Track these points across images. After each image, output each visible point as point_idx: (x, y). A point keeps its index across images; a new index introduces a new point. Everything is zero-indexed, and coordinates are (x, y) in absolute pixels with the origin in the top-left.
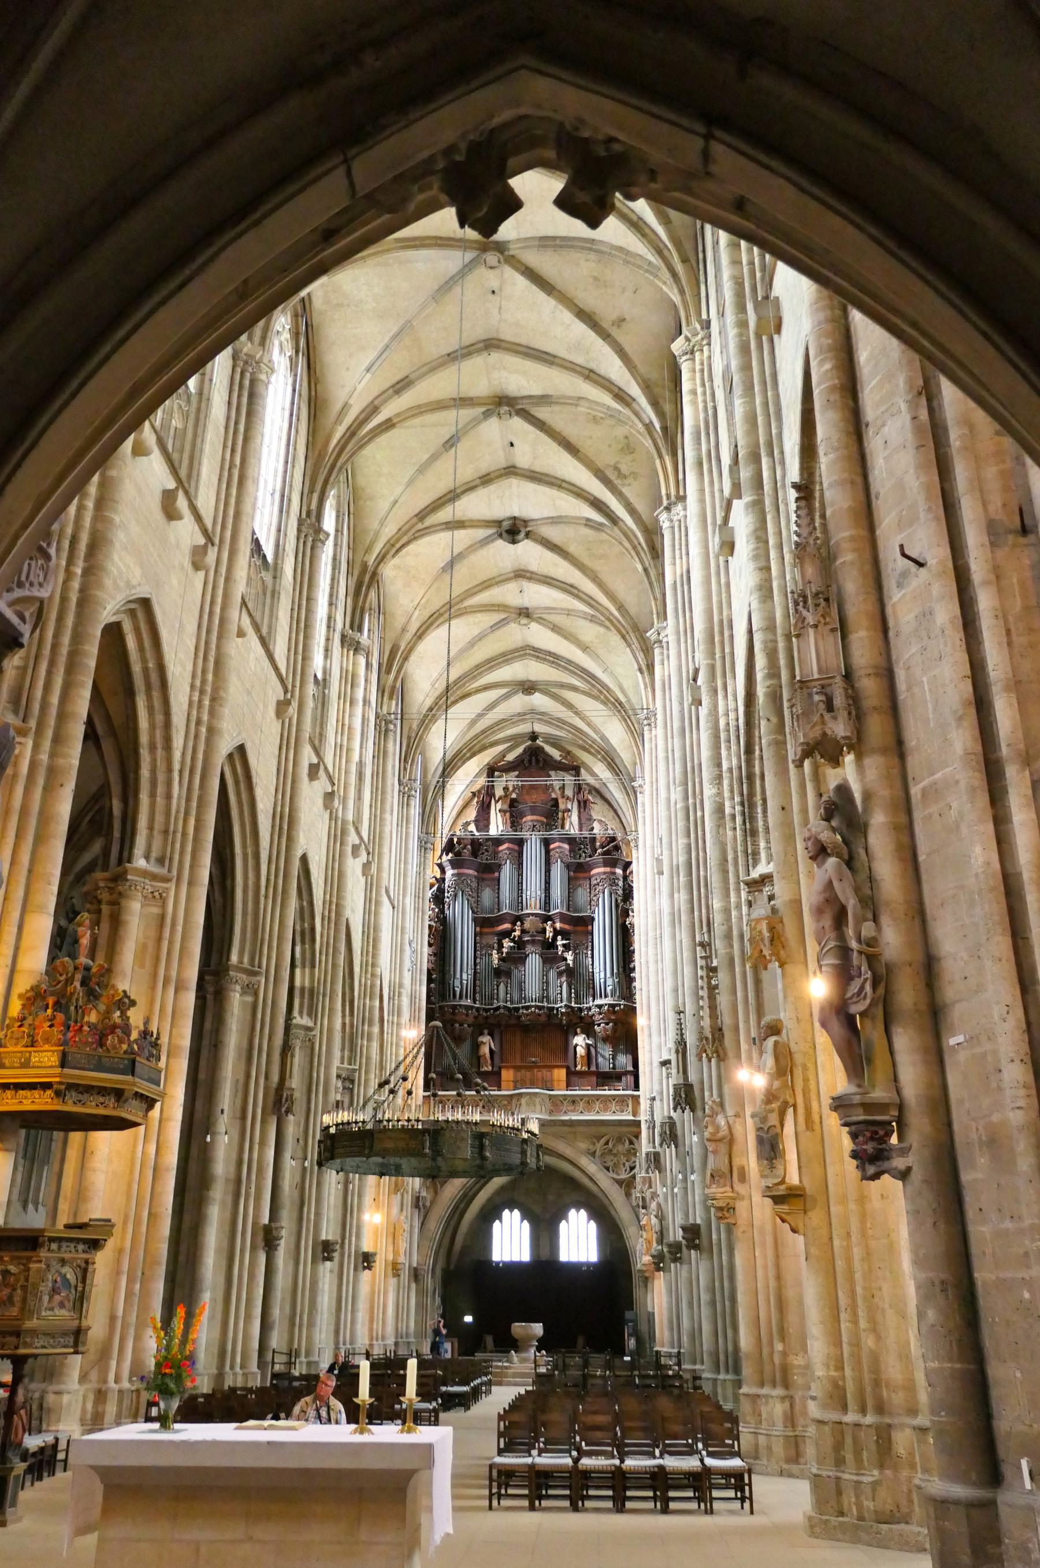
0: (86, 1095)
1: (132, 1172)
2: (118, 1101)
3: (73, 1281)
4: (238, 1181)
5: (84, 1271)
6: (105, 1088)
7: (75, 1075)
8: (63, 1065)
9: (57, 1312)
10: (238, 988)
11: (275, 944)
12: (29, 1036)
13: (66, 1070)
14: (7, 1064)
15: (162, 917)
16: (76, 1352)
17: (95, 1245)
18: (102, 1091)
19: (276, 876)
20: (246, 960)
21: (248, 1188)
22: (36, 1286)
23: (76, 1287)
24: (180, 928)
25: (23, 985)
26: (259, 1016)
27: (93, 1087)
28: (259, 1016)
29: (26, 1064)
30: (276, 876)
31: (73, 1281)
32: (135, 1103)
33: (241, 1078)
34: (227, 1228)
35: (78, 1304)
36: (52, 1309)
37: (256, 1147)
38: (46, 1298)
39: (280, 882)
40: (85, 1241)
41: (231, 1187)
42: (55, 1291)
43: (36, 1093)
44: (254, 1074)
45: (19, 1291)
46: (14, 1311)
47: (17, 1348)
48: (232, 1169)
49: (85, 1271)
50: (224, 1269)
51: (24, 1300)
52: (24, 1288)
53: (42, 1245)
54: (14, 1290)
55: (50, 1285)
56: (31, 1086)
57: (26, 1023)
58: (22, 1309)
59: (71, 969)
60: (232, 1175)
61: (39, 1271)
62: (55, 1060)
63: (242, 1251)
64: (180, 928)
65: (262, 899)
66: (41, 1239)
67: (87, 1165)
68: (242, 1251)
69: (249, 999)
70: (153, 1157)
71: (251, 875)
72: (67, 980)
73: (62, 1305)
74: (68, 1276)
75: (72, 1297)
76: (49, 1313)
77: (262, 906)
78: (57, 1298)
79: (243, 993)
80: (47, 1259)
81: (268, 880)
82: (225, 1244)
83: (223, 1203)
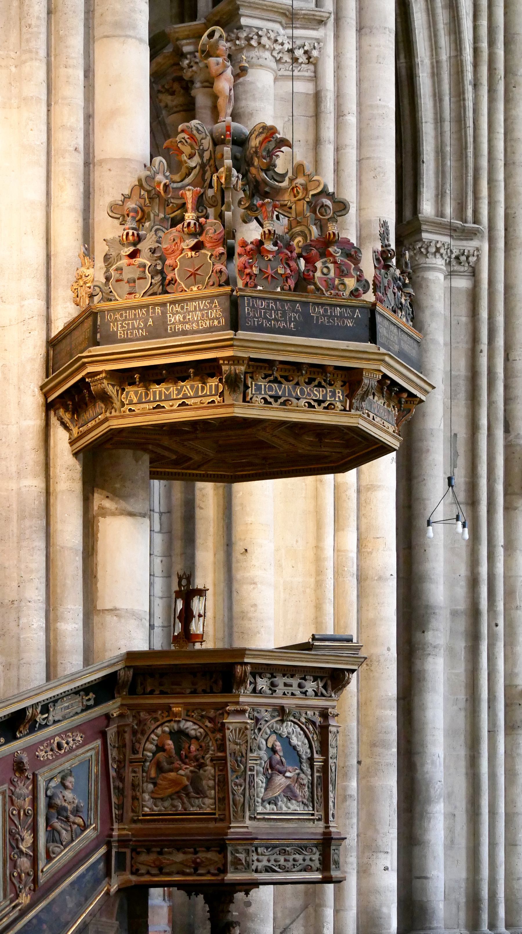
0: (287, 386)
1: (319, 584)
2: (350, 396)
3: (304, 750)
4: (474, 613)
5: (322, 731)
6: (322, 368)
7: (259, 343)
8: (235, 324)
9: (284, 806)
10: (439, 262)
11: (501, 176)
12: (155, 273)
13: (241, 334)
14: (120, 334)
15: (317, 98)
16: (327, 880)
17: (335, 680)
18: (317, 374)
19: (491, 43)
20: (449, 210)
21: (493, 625)
22: (241, 758)
23: (311, 760)
24: (352, 119)
25: (114, 186)
26: (484, 314)
27: (298, 366)
28: (484, 314)
29: (159, 330)
30: (491, 43)
31: (304, 750)
32: (378, 402)
33: (462, 433)
34: (462, 696)
35: (318, 793)
36: (273, 801)
37: (500, 552)
38: (260, 781)
39: (500, 52)
40: (317, 674)
41: (462, 624)
42: (273, 769)
43: (187, 387)
44: (484, 422)
45: (210, 769)
46: (207, 804)
47: (224, 871)
48: (461, 591)
49: (324, 731)
50: (462, 765)
51: (222, 783)
52: (220, 763)
53: (242, 682)
54: (201, 766)
55: (265, 756)
56: (177, 373)
57: (145, 246)
58: (223, 800)
59: (207, 143)
60: (462, 605)
61: (243, 730)
62: (217, 313)
63: (492, 732)
64: (352, 119)
65: (469, 89)
66: (239, 669)
67: (238, 575)
68: (492, 732)
69: (462, 283)
70: (353, 555)
71: (444, 40)
72: (203, 166)
73: (290, 794)
74: (294, 741)
75: (305, 780)
76: (269, 808)
77: (470, 104)
78: (280, 780)
79: (450, 274)
80: (255, 706)
81: (476, 51)
82: (461, 721)
83: (451, 651)
